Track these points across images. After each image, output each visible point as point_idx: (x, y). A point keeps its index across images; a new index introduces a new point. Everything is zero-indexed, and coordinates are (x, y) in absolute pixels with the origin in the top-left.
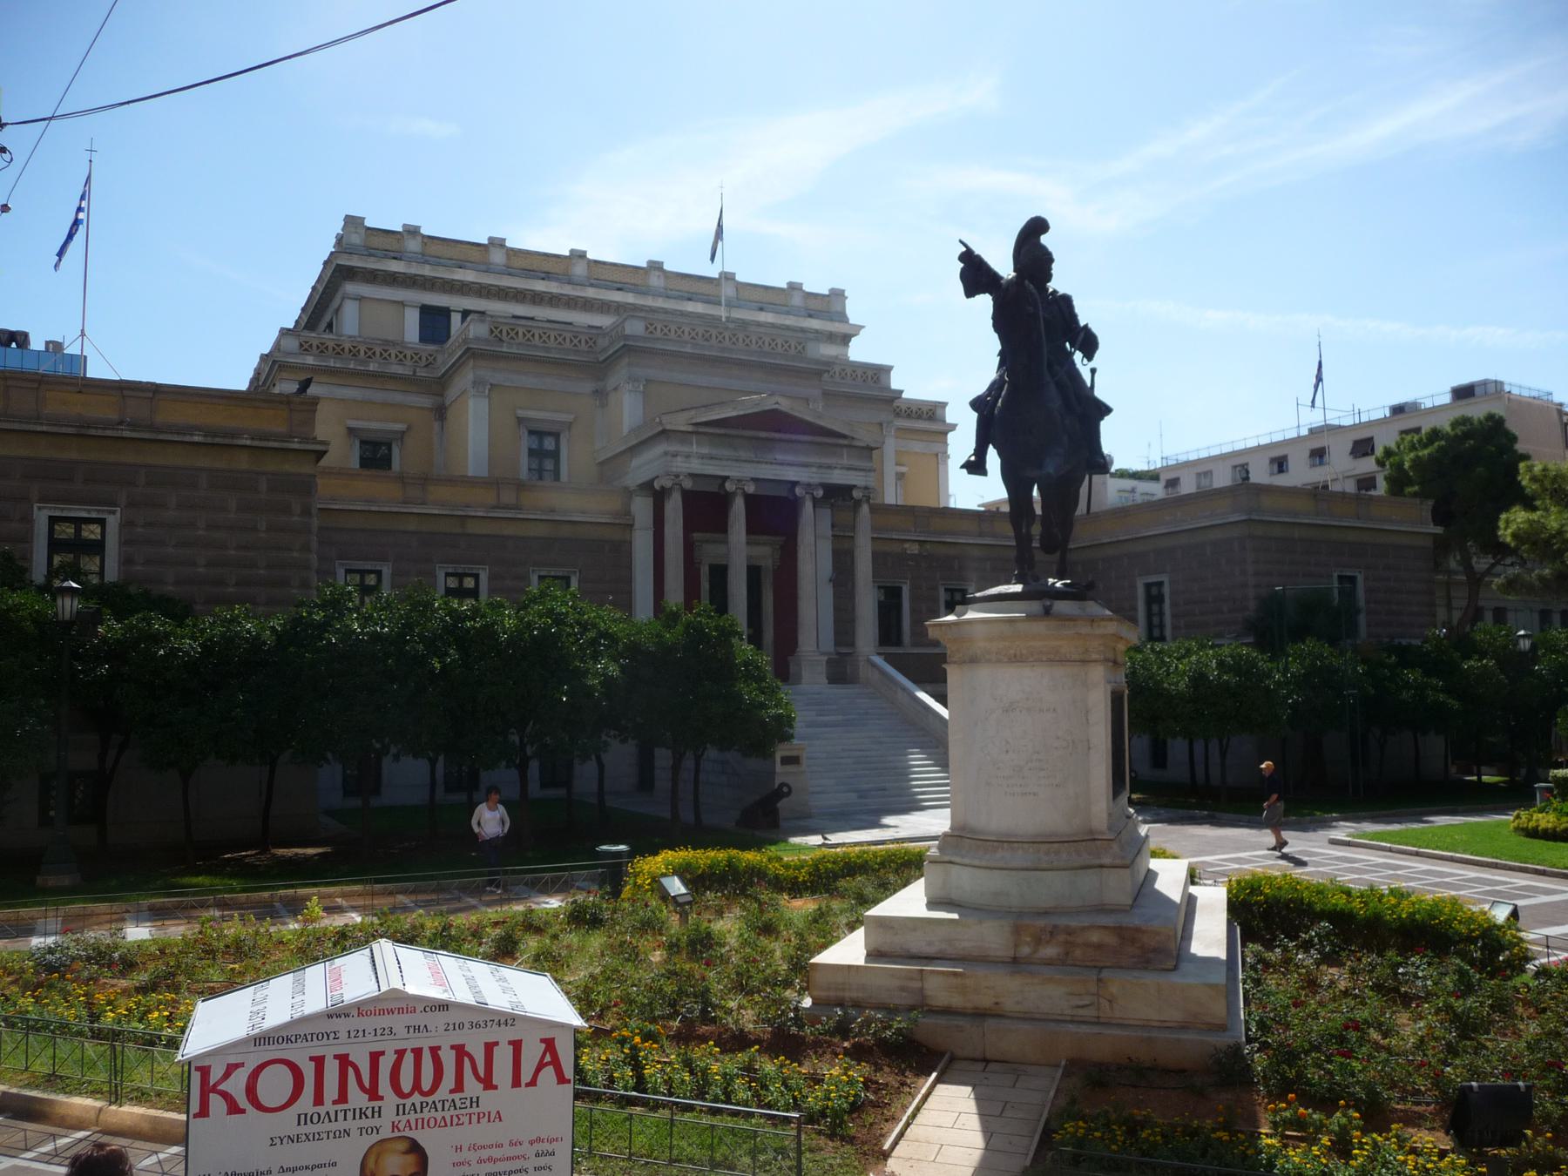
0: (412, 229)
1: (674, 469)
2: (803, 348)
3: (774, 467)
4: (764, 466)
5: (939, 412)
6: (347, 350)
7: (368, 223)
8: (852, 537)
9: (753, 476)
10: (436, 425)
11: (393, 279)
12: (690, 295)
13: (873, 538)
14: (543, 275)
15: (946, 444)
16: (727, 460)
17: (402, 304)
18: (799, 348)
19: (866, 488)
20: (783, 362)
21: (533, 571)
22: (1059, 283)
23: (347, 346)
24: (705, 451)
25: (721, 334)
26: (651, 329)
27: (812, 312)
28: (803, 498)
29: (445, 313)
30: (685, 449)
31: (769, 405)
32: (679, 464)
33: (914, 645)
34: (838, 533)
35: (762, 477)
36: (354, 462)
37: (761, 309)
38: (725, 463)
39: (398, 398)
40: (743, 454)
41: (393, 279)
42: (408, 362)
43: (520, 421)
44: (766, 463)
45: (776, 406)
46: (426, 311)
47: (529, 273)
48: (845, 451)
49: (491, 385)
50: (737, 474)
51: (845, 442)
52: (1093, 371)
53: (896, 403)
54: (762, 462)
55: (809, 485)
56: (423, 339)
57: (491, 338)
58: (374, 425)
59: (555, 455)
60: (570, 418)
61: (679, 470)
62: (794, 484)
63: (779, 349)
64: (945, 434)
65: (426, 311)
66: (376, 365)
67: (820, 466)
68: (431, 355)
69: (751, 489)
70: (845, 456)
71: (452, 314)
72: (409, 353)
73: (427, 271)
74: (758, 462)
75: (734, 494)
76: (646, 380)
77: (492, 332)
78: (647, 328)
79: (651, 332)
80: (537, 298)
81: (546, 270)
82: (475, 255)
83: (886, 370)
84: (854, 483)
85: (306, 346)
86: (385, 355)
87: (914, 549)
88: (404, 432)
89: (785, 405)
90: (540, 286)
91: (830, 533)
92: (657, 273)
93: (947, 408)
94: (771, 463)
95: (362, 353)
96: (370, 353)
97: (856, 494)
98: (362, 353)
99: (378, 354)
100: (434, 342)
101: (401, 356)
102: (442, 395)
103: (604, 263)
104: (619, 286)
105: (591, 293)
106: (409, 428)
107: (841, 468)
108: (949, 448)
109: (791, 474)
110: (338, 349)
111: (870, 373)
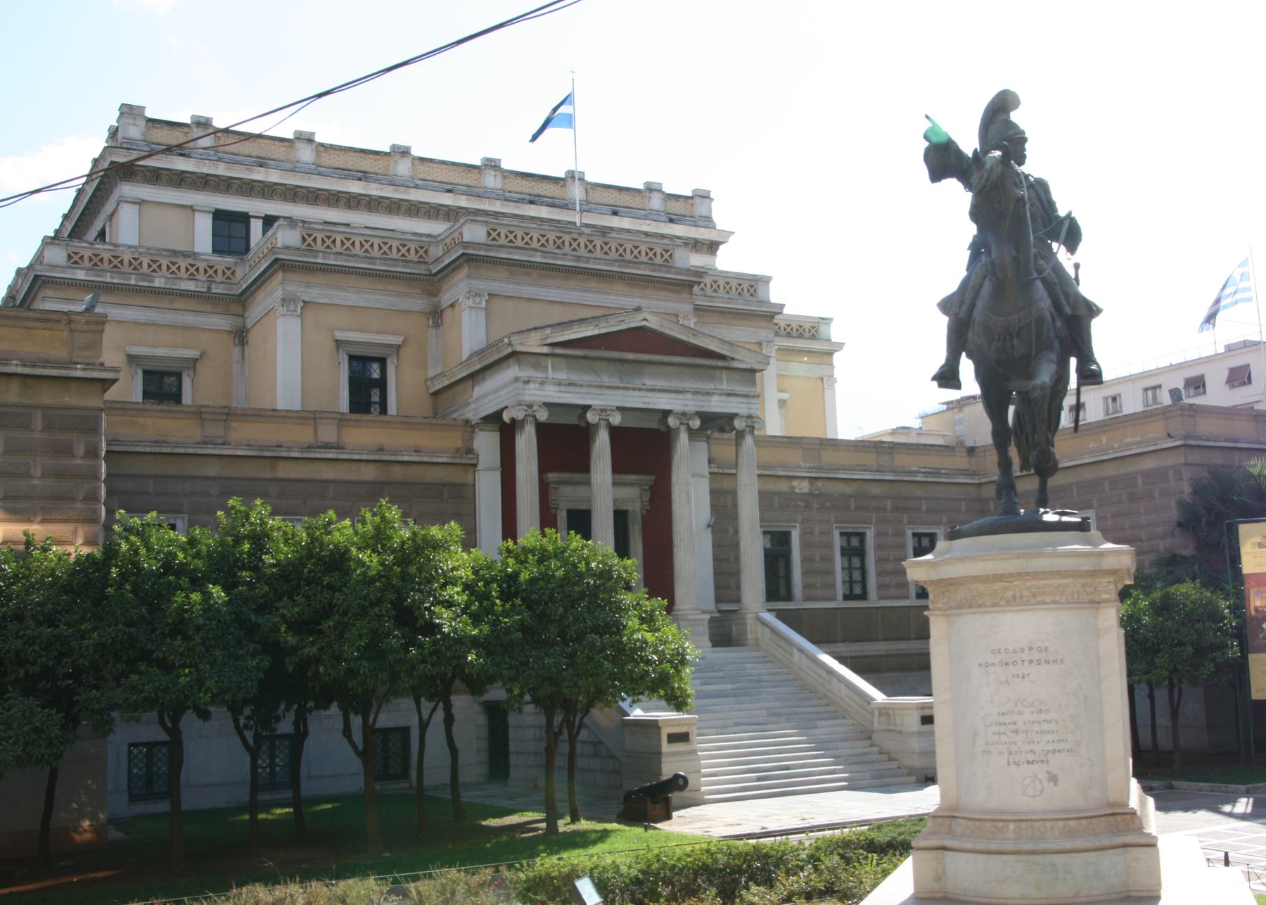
1: (527, 398)
2: (671, 256)
3: (643, 393)
4: (631, 393)
5: (823, 329)
6: (126, 262)
7: (150, 114)
8: (735, 475)
10: (236, 350)
11: (180, 180)
12: (532, 198)
13: (759, 475)
14: (360, 175)
15: (831, 365)
16: (589, 386)
17: (192, 209)
18: (666, 256)
19: (750, 417)
20: (648, 273)
22: (1033, 167)
23: (126, 257)
24: (562, 376)
25: (575, 240)
26: (494, 235)
28: (678, 429)
29: (244, 218)
30: (539, 375)
31: (635, 322)
32: (532, 391)
33: (807, 599)
34: (716, 470)
35: (629, 405)
36: (137, 396)
37: (615, 213)
38: (585, 390)
39: (189, 319)
40: (606, 380)
41: (180, 180)
42: (201, 277)
43: (339, 343)
44: (634, 389)
46: (220, 217)
47: (344, 173)
48: (724, 374)
49: (304, 302)
50: (601, 403)
52: (1077, 266)
53: (777, 319)
54: (628, 389)
55: (684, 414)
56: (216, 250)
57: (304, 247)
59: (382, 384)
61: (533, 398)
62: (666, 413)
63: (643, 258)
64: (830, 354)
65: (220, 217)
66: (163, 280)
68: (228, 269)
70: (725, 382)
71: (252, 220)
72: (202, 266)
73: (221, 170)
74: (624, 388)
75: (596, 426)
76: (489, 294)
77: (304, 240)
78: (489, 234)
79: (494, 239)
80: (353, 201)
81: (363, 169)
82: (278, 152)
83: (766, 281)
85: (76, 258)
86: (174, 268)
88: (197, 360)
89: (653, 323)
90: (355, 187)
91: (705, 469)
92: (493, 173)
94: (640, 389)
95: (145, 265)
96: (155, 266)
97: (738, 424)
98: (145, 265)
99: (164, 267)
100: (229, 252)
101: (192, 270)
102: (243, 316)
103: (431, 161)
104: (449, 187)
105: (415, 195)
106: (203, 354)
107: (721, 394)
108: (836, 370)
110: (116, 262)
111: (745, 285)
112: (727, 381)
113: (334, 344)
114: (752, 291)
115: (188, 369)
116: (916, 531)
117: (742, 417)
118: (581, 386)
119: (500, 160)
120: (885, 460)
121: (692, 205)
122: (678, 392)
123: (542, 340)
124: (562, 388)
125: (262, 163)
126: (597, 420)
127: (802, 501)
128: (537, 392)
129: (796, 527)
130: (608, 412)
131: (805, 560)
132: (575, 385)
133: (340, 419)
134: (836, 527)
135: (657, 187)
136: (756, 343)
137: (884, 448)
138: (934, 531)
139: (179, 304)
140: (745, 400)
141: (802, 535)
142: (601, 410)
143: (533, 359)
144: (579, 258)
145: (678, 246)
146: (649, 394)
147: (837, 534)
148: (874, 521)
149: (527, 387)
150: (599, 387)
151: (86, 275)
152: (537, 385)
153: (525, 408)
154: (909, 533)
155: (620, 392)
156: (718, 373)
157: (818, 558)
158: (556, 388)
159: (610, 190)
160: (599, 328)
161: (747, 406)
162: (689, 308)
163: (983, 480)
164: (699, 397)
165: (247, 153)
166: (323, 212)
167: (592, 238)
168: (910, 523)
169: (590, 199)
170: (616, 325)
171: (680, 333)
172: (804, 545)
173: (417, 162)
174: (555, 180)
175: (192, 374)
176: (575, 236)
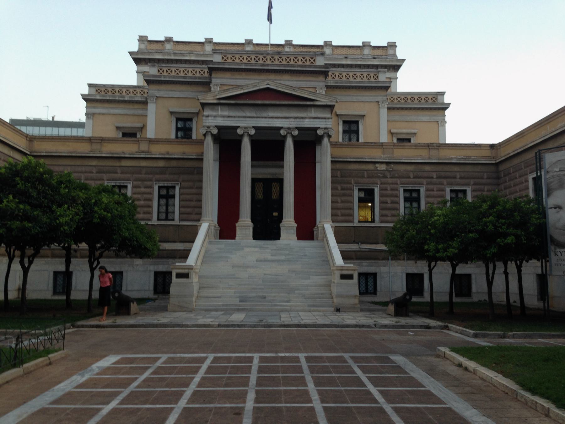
0: (168, 39)
2: (314, 60)
3: (267, 119)
5: (439, 98)
6: (117, 91)
7: (150, 39)
9: (254, 125)
19: (326, 128)
21: (155, 183)
24: (226, 113)
25: (264, 57)
27: (376, 56)
30: (214, 113)
32: (210, 121)
33: (382, 222)
38: (237, 119)
40: (248, 114)
43: (172, 113)
44: (262, 117)
45: (268, 86)
48: (313, 109)
49: (157, 97)
51: (311, 103)
55: (289, 128)
58: (130, 123)
61: (211, 124)
69: (253, 132)
75: (242, 136)
78: (223, 58)
84: (318, 126)
87: (383, 167)
93: (445, 96)
94: (265, 118)
95: (124, 92)
98: (124, 92)
109: (277, 123)
112: (314, 112)
113: (170, 114)
114: (375, 77)
115: (139, 131)
116: (452, 189)
117: (322, 128)
118: (235, 117)
119: (292, 41)
121: (386, 50)
123: (214, 96)
124: (225, 119)
125: (191, 53)
126: (242, 132)
127: (381, 174)
128: (212, 121)
129: (377, 186)
130: (248, 129)
131: (381, 202)
132: (231, 117)
133: (150, 141)
134: (401, 187)
135: (368, 44)
136: (377, 102)
137: (434, 146)
138: (465, 188)
139: (136, 106)
140: (324, 120)
141: (381, 189)
142: (245, 128)
144: (268, 65)
145: (318, 55)
146: (270, 120)
147: (402, 191)
148: (425, 183)
149: (208, 118)
150: (244, 117)
151: (100, 97)
152: (213, 118)
153: (206, 128)
154: (448, 190)
155: (255, 119)
156: (309, 109)
157: (389, 202)
158: (222, 119)
159: (344, 48)
160: (244, 90)
161: (325, 123)
162: (323, 84)
163: (497, 161)
164: (298, 120)
165: (186, 50)
167: (273, 56)
168: (448, 184)
169: (334, 53)
170: (252, 88)
171: (287, 90)
172: (381, 196)
173: (256, 46)
175: (140, 133)
176: (265, 55)
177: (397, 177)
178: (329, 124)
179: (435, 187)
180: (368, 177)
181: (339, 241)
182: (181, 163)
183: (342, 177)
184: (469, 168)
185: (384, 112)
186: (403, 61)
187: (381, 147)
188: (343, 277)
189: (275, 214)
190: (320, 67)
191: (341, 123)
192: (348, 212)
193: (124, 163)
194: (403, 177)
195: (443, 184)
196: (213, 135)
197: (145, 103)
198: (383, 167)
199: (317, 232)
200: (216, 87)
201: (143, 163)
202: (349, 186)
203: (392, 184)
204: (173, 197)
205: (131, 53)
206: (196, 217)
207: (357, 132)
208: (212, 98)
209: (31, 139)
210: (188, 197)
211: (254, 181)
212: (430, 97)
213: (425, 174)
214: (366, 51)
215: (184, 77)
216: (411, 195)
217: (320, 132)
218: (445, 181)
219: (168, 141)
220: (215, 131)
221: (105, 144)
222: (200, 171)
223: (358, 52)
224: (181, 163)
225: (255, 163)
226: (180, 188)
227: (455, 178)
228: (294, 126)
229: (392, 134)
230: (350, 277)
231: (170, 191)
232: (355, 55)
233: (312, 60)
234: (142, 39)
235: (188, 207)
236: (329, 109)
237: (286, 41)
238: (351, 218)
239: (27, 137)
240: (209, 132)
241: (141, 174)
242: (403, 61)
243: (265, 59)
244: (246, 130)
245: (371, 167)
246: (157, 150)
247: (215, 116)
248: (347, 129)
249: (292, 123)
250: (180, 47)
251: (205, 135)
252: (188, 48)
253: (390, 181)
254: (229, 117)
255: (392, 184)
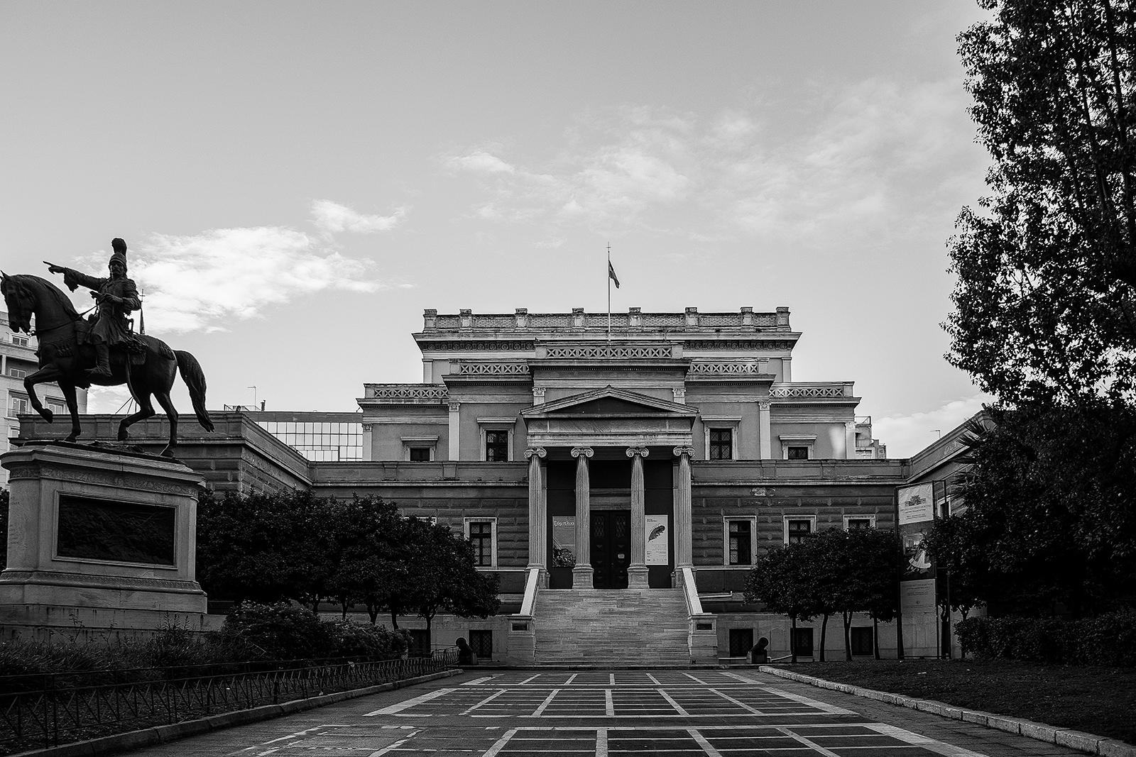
1: (533, 445)
5: (847, 389)
6: (402, 393)
16: (572, 435)
26: (551, 353)
39: (434, 420)
43: (480, 425)
44: (603, 435)
50: (581, 445)
54: (599, 435)
55: (637, 448)
58: (420, 437)
60: (512, 420)
61: (537, 445)
67: (645, 434)
78: (548, 353)
87: (763, 493)
88: (437, 441)
94: (607, 435)
95: (411, 393)
96: (416, 393)
98: (411, 393)
103: (596, 315)
107: (663, 434)
120: (827, 471)
122: (632, 435)
124: (556, 438)
131: (759, 539)
141: (759, 522)
142: (581, 449)
143: (539, 423)
144: (608, 360)
146: (613, 438)
147: (786, 523)
154: (846, 520)
156: (663, 421)
158: (551, 438)
166: (530, 353)
169: (701, 324)
172: (759, 530)
174: (678, 315)
177: (780, 505)
178: (688, 441)
179: (830, 517)
180: (743, 506)
181: (700, 591)
182: (497, 493)
183: (707, 506)
184: (873, 492)
185: (766, 416)
186: (799, 334)
187: (759, 466)
188: (700, 626)
189: (621, 556)
190: (677, 361)
191: (708, 433)
192: (714, 551)
193: (426, 494)
194: (788, 505)
195: (839, 513)
196: (543, 462)
197: (443, 409)
198: (763, 493)
199: (675, 579)
200: (540, 392)
201: (450, 494)
202: (716, 518)
203: (774, 514)
204: (489, 536)
205: (415, 336)
206: (522, 561)
207: (730, 443)
208: (538, 412)
209: (312, 466)
210: (507, 536)
211: (594, 514)
212: (834, 389)
213: (817, 501)
214: (747, 320)
215: (496, 376)
216: (799, 528)
217: (676, 452)
218: (843, 509)
219: (478, 465)
220: (543, 454)
221: (401, 470)
222: (524, 503)
223: (735, 321)
224: (497, 493)
225: (595, 491)
226: (497, 525)
227: (856, 504)
228: (644, 445)
229: (781, 441)
230: (708, 627)
231: (484, 529)
232: (731, 326)
233: (666, 352)
234: (429, 314)
235: (509, 549)
236: (688, 422)
237: (631, 309)
238: (719, 560)
239: (307, 464)
240: (536, 454)
241: (448, 508)
242: (799, 334)
243: (603, 353)
244: (582, 452)
245: (746, 492)
246: (468, 477)
247: (543, 435)
248: (716, 439)
249: (642, 442)
250: (482, 322)
251: (530, 459)
252: (493, 323)
253: (772, 510)
254: (560, 435)
255: (774, 514)
